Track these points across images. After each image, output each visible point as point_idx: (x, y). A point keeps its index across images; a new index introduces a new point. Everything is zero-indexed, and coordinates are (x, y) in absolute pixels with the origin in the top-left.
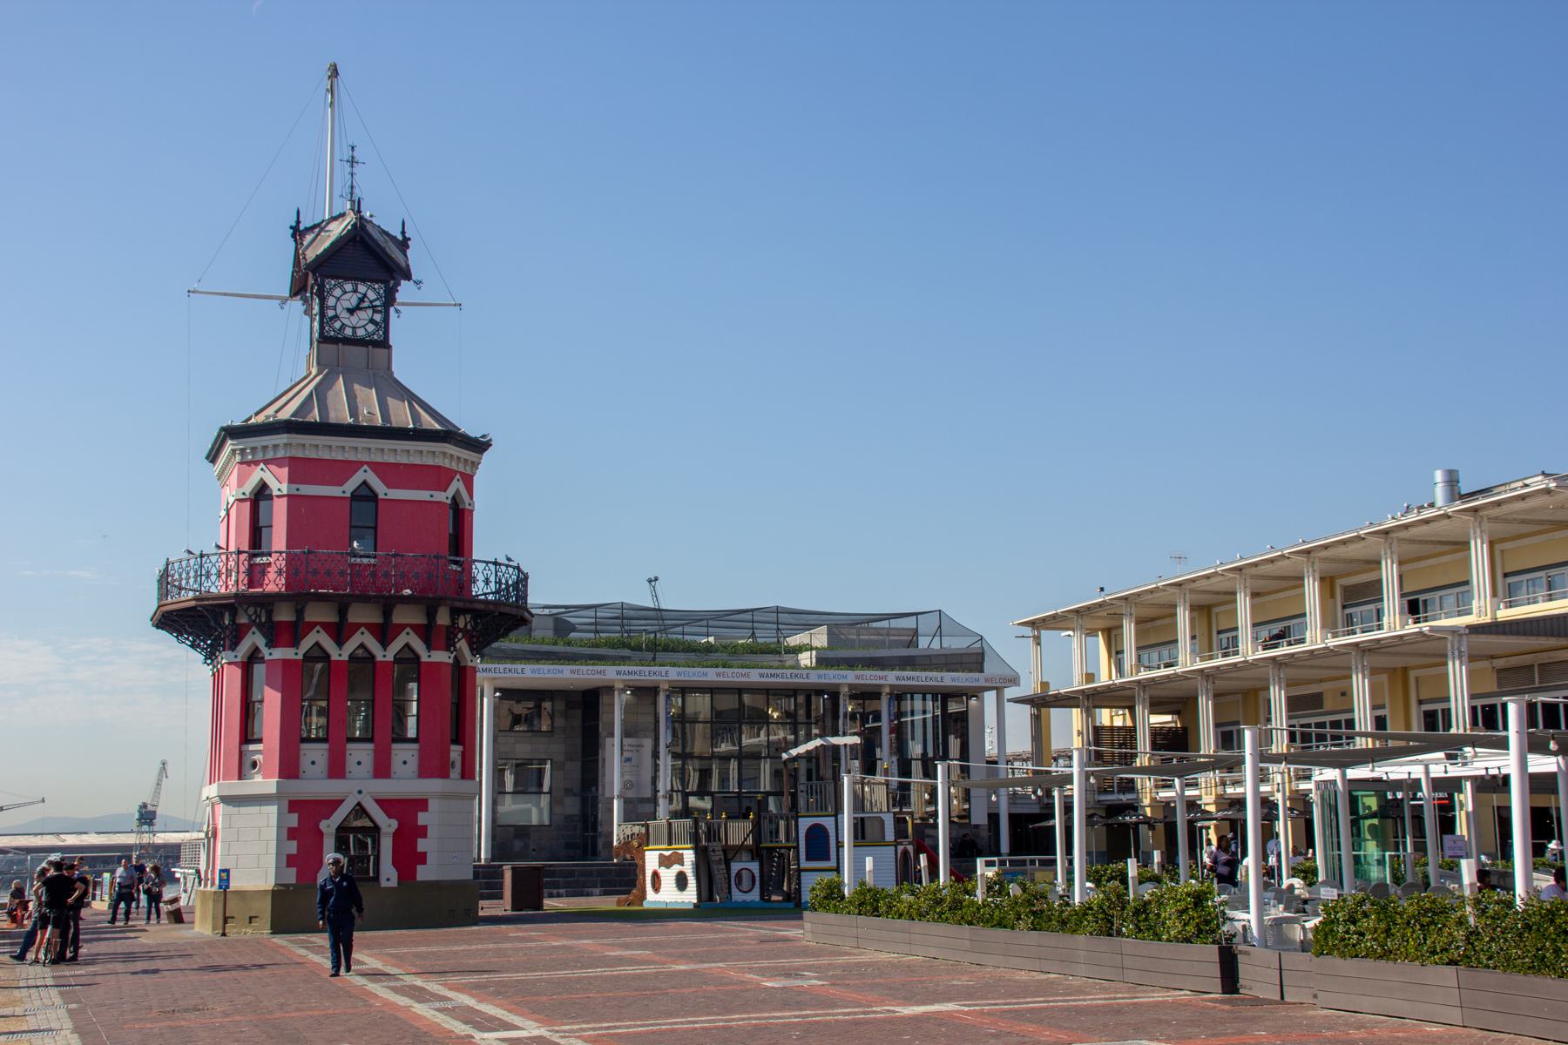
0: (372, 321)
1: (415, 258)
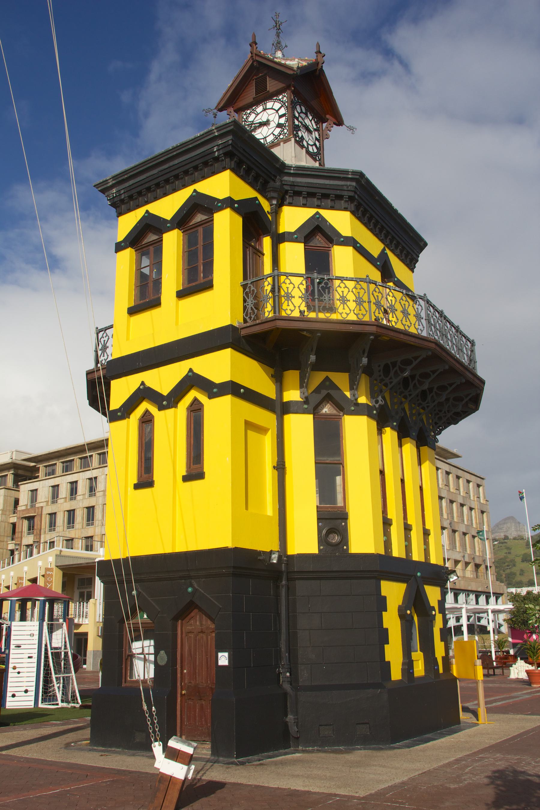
0: (279, 125)
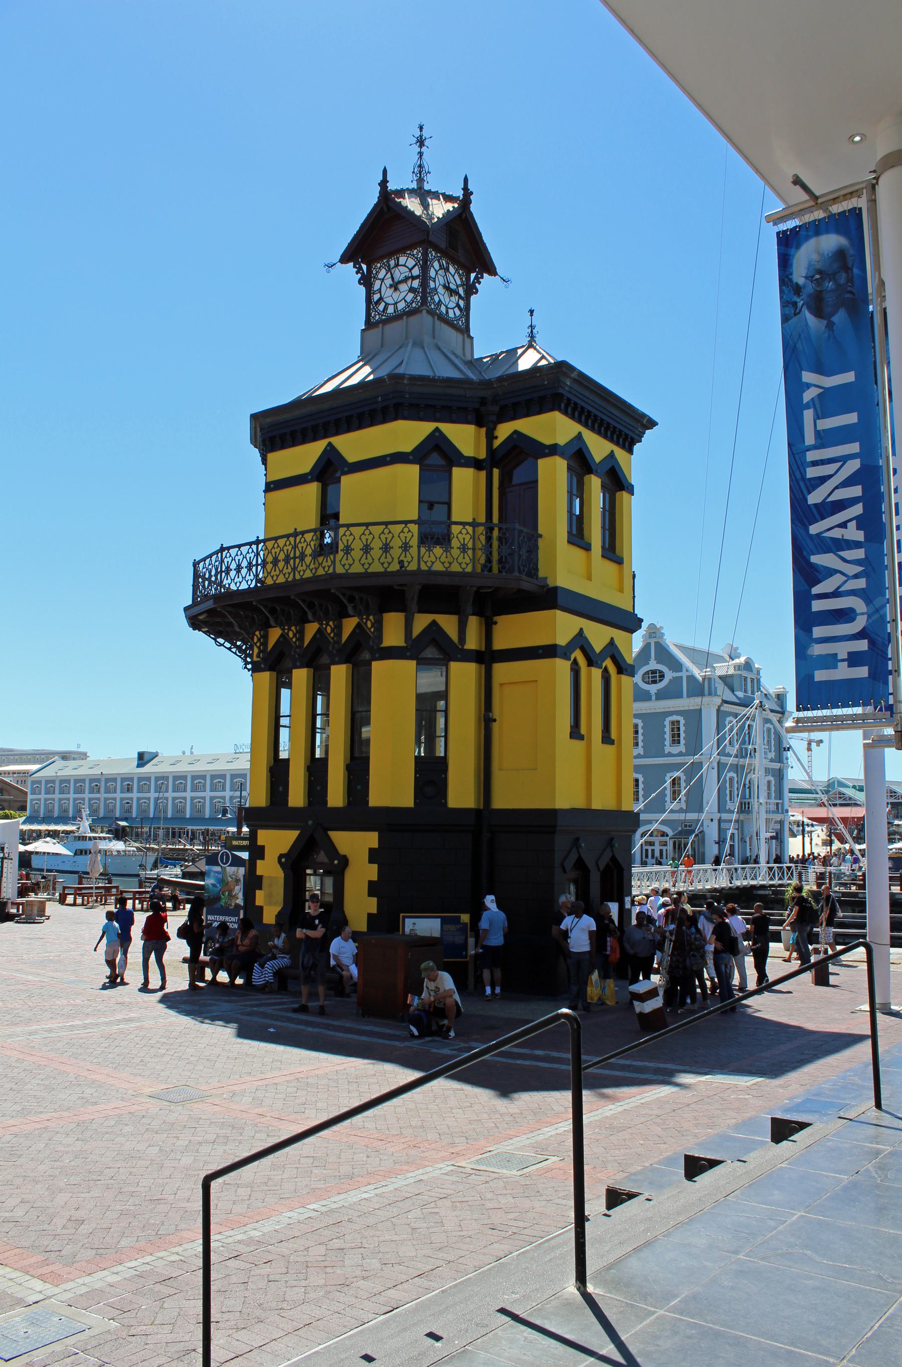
0: (412, 290)
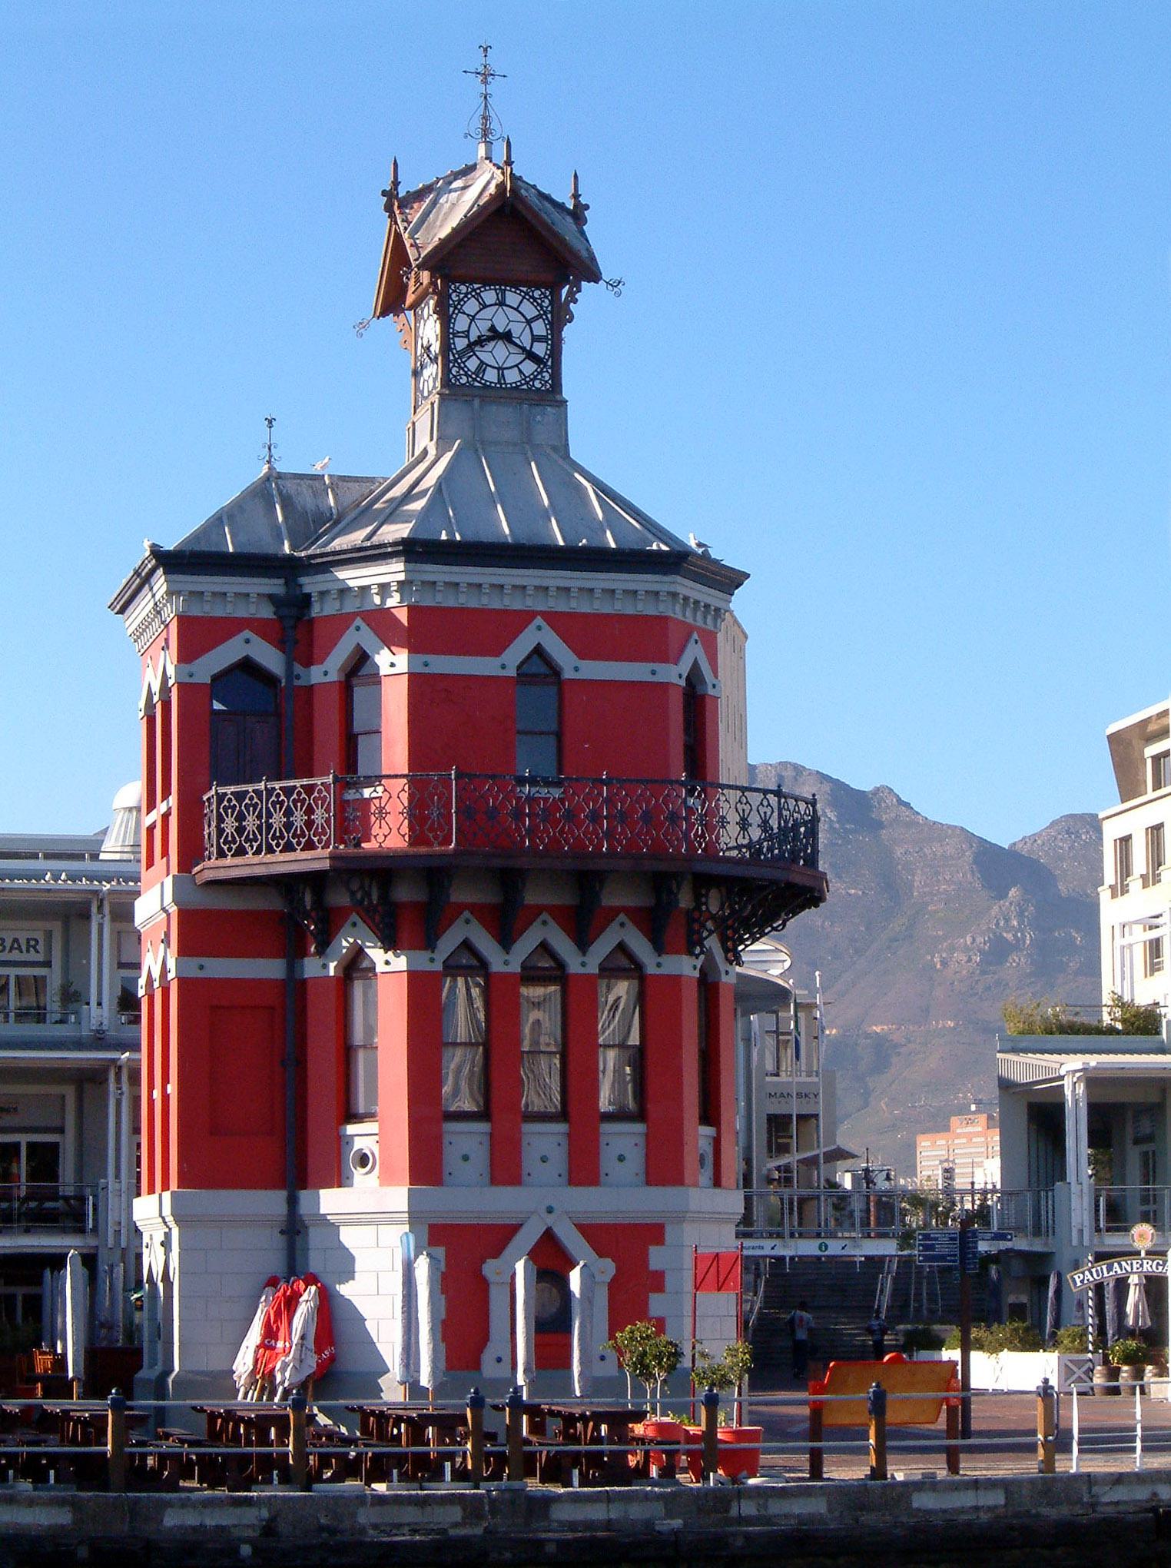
1: (602, 237)
